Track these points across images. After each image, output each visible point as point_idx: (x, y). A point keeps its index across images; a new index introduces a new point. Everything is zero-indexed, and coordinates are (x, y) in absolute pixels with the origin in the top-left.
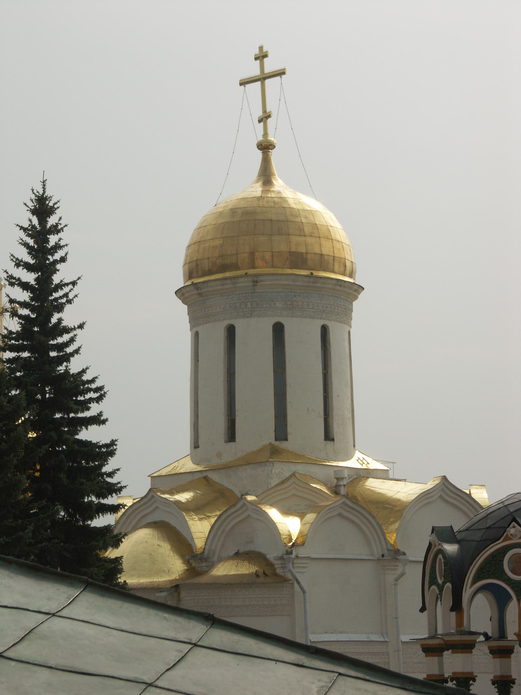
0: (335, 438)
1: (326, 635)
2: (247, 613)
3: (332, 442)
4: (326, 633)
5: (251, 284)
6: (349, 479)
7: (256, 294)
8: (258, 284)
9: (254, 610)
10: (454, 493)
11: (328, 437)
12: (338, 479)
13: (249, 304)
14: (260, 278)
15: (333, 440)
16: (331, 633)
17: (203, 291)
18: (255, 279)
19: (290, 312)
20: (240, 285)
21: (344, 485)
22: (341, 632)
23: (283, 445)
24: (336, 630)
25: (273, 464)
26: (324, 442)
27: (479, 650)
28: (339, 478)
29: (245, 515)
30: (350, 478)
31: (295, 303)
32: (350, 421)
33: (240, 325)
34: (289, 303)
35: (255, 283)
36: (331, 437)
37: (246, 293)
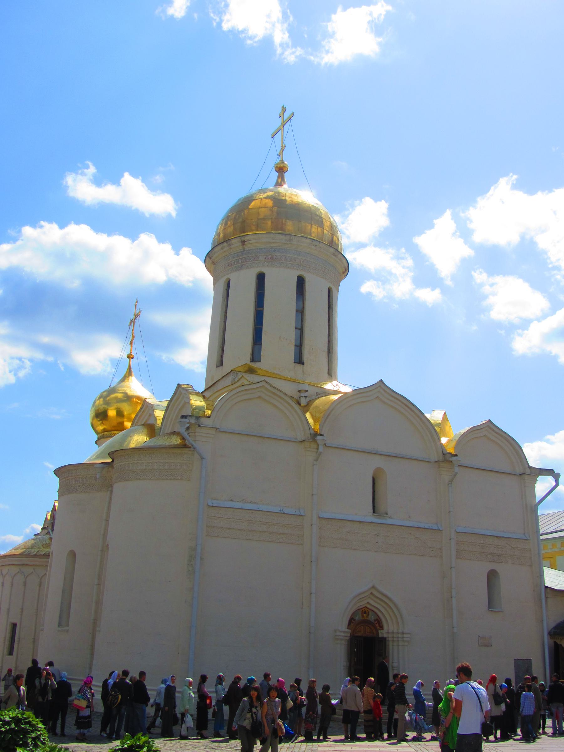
0: (305, 362)
1: (231, 502)
2: (149, 476)
3: (302, 365)
4: (232, 500)
5: (241, 244)
6: (316, 396)
7: (245, 252)
8: (246, 243)
9: (155, 474)
10: (392, 396)
11: (299, 360)
12: (299, 391)
13: (240, 260)
14: (247, 238)
15: (303, 364)
16: (238, 502)
17: (213, 258)
18: (243, 239)
19: (271, 263)
20: (232, 246)
21: (305, 396)
22: (250, 502)
23: (255, 365)
24: (244, 500)
25: (237, 374)
26: (294, 364)
27: (410, 533)
28: (301, 390)
29: (183, 402)
30: (318, 395)
31: (275, 257)
32: (325, 354)
33: (233, 277)
34: (269, 257)
35: (243, 242)
36: (302, 362)
37: (238, 253)
